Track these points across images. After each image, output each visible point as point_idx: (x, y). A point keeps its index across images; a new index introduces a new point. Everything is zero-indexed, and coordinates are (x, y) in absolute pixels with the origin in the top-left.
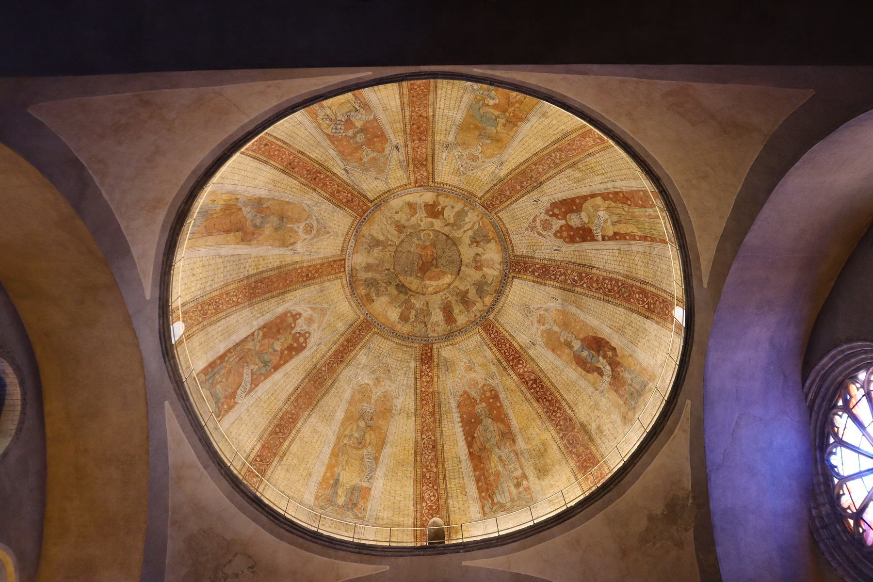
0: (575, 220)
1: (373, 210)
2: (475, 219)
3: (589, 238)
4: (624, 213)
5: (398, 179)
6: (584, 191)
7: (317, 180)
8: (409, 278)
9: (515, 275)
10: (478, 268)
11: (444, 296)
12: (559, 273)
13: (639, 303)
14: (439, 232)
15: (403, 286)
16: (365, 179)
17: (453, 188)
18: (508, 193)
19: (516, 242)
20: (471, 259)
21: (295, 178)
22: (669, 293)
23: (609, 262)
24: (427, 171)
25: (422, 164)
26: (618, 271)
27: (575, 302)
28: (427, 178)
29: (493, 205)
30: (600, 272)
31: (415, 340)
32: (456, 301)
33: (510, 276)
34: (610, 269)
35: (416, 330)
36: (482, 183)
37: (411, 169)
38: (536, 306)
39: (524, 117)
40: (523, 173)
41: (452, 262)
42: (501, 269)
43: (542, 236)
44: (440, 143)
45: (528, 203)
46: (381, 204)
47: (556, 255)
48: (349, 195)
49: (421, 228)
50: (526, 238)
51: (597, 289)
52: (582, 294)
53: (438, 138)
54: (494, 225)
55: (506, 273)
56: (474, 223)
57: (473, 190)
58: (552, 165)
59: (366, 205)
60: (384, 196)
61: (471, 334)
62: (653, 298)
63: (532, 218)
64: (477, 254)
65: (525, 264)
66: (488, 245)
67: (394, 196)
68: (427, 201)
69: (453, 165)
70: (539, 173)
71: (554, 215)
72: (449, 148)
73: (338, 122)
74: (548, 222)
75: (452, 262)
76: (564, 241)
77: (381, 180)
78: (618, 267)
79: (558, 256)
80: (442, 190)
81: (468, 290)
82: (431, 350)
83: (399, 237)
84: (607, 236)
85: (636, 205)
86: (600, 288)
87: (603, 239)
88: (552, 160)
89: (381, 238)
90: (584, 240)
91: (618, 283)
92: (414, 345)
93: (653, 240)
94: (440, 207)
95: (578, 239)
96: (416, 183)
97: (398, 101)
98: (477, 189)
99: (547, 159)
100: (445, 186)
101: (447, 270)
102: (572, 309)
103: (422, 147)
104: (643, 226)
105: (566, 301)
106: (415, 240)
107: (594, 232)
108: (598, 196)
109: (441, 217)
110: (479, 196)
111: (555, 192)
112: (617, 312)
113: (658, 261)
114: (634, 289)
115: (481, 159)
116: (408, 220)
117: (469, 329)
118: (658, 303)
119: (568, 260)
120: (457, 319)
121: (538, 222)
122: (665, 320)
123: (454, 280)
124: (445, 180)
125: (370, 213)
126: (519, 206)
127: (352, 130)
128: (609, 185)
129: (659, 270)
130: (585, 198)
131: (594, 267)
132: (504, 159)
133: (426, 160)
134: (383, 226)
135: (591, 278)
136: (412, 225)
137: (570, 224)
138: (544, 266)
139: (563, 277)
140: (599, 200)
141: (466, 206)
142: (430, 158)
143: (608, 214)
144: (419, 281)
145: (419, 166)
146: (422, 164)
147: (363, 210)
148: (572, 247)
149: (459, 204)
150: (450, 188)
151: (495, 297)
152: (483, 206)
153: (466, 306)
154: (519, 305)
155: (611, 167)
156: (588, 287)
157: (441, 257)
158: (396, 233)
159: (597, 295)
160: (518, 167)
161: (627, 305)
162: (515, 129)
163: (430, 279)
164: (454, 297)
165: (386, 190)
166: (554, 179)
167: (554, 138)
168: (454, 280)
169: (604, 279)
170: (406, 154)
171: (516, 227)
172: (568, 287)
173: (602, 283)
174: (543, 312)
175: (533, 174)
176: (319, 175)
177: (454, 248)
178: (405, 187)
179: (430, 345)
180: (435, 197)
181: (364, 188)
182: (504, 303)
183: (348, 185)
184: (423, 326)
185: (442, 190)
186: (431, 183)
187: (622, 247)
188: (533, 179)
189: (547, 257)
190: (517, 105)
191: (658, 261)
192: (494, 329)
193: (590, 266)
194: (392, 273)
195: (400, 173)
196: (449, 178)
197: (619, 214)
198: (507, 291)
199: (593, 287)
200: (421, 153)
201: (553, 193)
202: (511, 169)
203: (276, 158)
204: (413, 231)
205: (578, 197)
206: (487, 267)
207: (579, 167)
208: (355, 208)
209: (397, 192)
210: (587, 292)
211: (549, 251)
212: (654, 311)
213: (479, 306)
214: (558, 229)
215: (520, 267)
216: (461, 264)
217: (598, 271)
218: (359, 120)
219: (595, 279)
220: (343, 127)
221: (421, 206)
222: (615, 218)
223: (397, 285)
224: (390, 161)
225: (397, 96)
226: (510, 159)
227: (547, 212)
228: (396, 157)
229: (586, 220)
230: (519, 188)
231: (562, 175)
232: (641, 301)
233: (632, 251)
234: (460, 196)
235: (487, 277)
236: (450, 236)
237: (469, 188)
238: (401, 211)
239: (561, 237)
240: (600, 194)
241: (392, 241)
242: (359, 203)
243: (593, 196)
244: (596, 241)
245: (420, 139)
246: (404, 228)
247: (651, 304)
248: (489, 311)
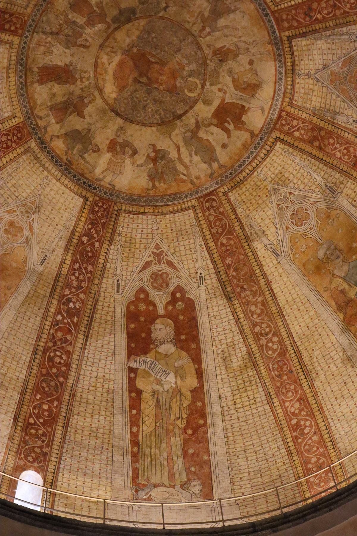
0: (164, 332)
1: (274, 32)
2: (194, 172)
3: (133, 345)
4: (172, 417)
5: (307, 94)
8: (137, 33)
9: (88, 203)
10: (113, 146)
11: (86, 75)
12: (81, 277)
13: (34, 408)
14: (191, 108)
15: (129, 20)
16: (334, 52)
17: (256, 161)
18: (224, 241)
19: (140, 221)
20: (129, 139)
22: (59, 468)
23: (94, 369)
24: (301, 140)
25: (315, 138)
26: (81, 381)
27: (37, 294)
28: (289, 134)
29: (208, 209)
30: (79, 350)
31: (38, 10)
32: (72, 93)
33: (88, 195)
34: (83, 367)
35: (52, 17)
36: (251, 208)
37: (315, 120)
38: (35, 225)
39: (352, 328)
40: (252, 278)
41: (134, 108)
42: (102, 183)
43: (144, 268)
44: (341, 183)
45: (199, 264)
46: (278, 49)
47: (111, 281)
48: (319, 16)
49: (208, 84)
50: (144, 241)
51: (54, 337)
52: (47, 310)
54: (175, 197)
55: (95, 188)
56: (186, 167)
57: (244, 189)
58: (257, 329)
59: (289, 29)
60: (289, 60)
61: (14, 103)
62: (44, 435)
63: (175, 262)
64: (135, 152)
65: (104, 224)
66: (145, 175)
67: (281, 73)
68: (249, 114)
69: (295, 181)
70: (248, 303)
71: (173, 300)
72: (327, 191)
74: (164, 285)
75: (134, 108)
76: (132, 302)
77: (318, 71)
78: (86, 383)
79: (107, 284)
80: (259, 144)
81: (83, 117)
82: (12, 31)
83: (209, 46)
84: (135, 378)
85: (186, 442)
86: (55, 343)
87: (131, 370)
88: (267, 334)
89: (222, 22)
90: (131, 336)
91: (63, 377)
92: (31, 5)
93: (135, 457)
94: (231, 127)
95: (132, 326)
96: (288, 114)
98: (243, 197)
99: (269, 326)
100: (264, 152)
101: (125, 95)
102: (25, 287)
103: (344, 155)
104: (154, 444)
105: (39, 279)
106: (193, 66)
107: (142, 358)
108: (199, 382)
109: (215, 121)
110: (230, 194)
111: (212, 315)
112: (20, 365)
113: (103, 457)
114: (56, 403)
116: (230, 72)
117: (24, 101)
118: (39, 443)
119: (101, 299)
120: (44, 86)
121: (166, 268)
122: (18, 452)
123: (105, 101)
124: (274, 158)
125: (272, 27)
126: (198, 247)
128: (216, 407)
129: (90, 456)
131: (87, 341)
132: (284, 261)
133: (320, 148)
134: (240, 33)
135: (70, 331)
136: (219, 73)
137: (158, 321)
138: (95, 256)
139: (75, 283)
140: (192, 382)
141: (221, 167)
142: (321, 155)
143: (171, 391)
144: (125, 46)
145: (315, 134)
146: (315, 138)
147: (283, 20)
148: (120, 312)
149: (227, 158)
150: (259, 158)
151: (61, 159)
152: (211, 193)
153: (60, 106)
154: (42, 197)
155: (246, 421)
156: (57, 322)
157: (149, 93)
158: (219, 45)
159: (44, 336)
160: (265, 276)
161: (30, 385)
162: (333, 304)
163: (121, 65)
164: (78, 92)
165: (297, 68)
166: (233, 322)
168: (105, 101)
169: (69, 354)
170: (346, 128)
171: (164, 231)
172: (59, 288)
173: (62, 348)
174: (25, 236)
175: (248, 293)
177: (156, 119)
178: (288, 95)
179: (20, 31)
180: (251, 128)
181: (319, 42)
182: (49, 172)
183: (337, 26)
184: (54, 29)
185: (259, 144)
186: (277, 134)
187: (118, 398)
188: (238, 290)
189: (108, 265)
191: (103, 457)
192: (14, 145)
193: (88, 333)
194: (158, 12)
195: (316, 102)
196: (276, 165)
197: (170, 408)
198: (66, 182)
199: (56, 331)
200: (336, 148)
201: (210, 310)
202: (264, 263)
204: (209, 70)
205: (198, 349)
206: (110, 162)
207: (249, 370)
208: (294, 12)
209: (286, 81)
210: (50, 319)
211: (118, 272)
212: (26, 434)
213: (54, 128)
214: (151, 298)
215: (99, 214)
216: (126, 119)
217: (80, 346)
219: (69, 337)
221: (245, 101)
222: (163, 399)
223: (133, 11)
224: (344, 101)
226: (281, 271)
227: (179, 289)
229: (162, 349)
231: (238, 337)
232: (39, 413)
233: (112, 414)
234: (240, 166)
235: (95, 155)
236: (178, 122)
237: (248, 186)
238: (251, 69)
239: (137, 298)
240: (202, 387)
241: (209, 34)
242: (297, 21)
243: (200, 374)
244: (129, 357)
246: (220, 61)
247: (37, 430)
248: (42, 143)
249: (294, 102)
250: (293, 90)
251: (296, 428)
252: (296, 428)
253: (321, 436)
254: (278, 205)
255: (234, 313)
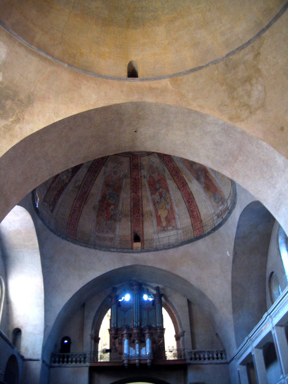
6: (73, 180)
7: (176, 171)
21: (183, 177)
28: (133, 159)
44: (128, 177)
48: (165, 158)
53: (129, 180)
58: (86, 182)
73: (164, 198)
96: (137, 157)
97: (143, 203)
115: (112, 173)
127: (160, 191)
130: (72, 177)
133: (133, 169)
140: (67, 181)
145: (136, 166)
146: (135, 166)
165: (150, 155)
167: (89, 197)
176: (175, 174)
181: (158, 159)
186: (131, 156)
190: (104, 208)
195: (144, 163)
203: (188, 193)
205: (74, 175)
209: (145, 154)
218: (157, 197)
220: (163, 194)
225: (143, 206)
228: (144, 173)
230: (96, 164)
231: (82, 180)
243: (70, 181)
245: (136, 179)
249: (141, 158)
250: (144, 156)
251: (75, 210)
252: (75, 210)
253: (77, 218)
254: (115, 166)
255: (86, 174)
